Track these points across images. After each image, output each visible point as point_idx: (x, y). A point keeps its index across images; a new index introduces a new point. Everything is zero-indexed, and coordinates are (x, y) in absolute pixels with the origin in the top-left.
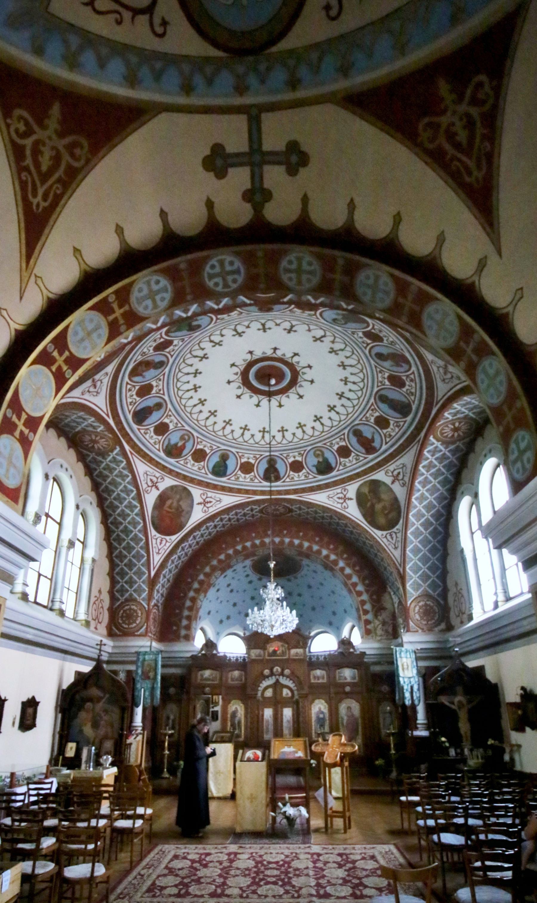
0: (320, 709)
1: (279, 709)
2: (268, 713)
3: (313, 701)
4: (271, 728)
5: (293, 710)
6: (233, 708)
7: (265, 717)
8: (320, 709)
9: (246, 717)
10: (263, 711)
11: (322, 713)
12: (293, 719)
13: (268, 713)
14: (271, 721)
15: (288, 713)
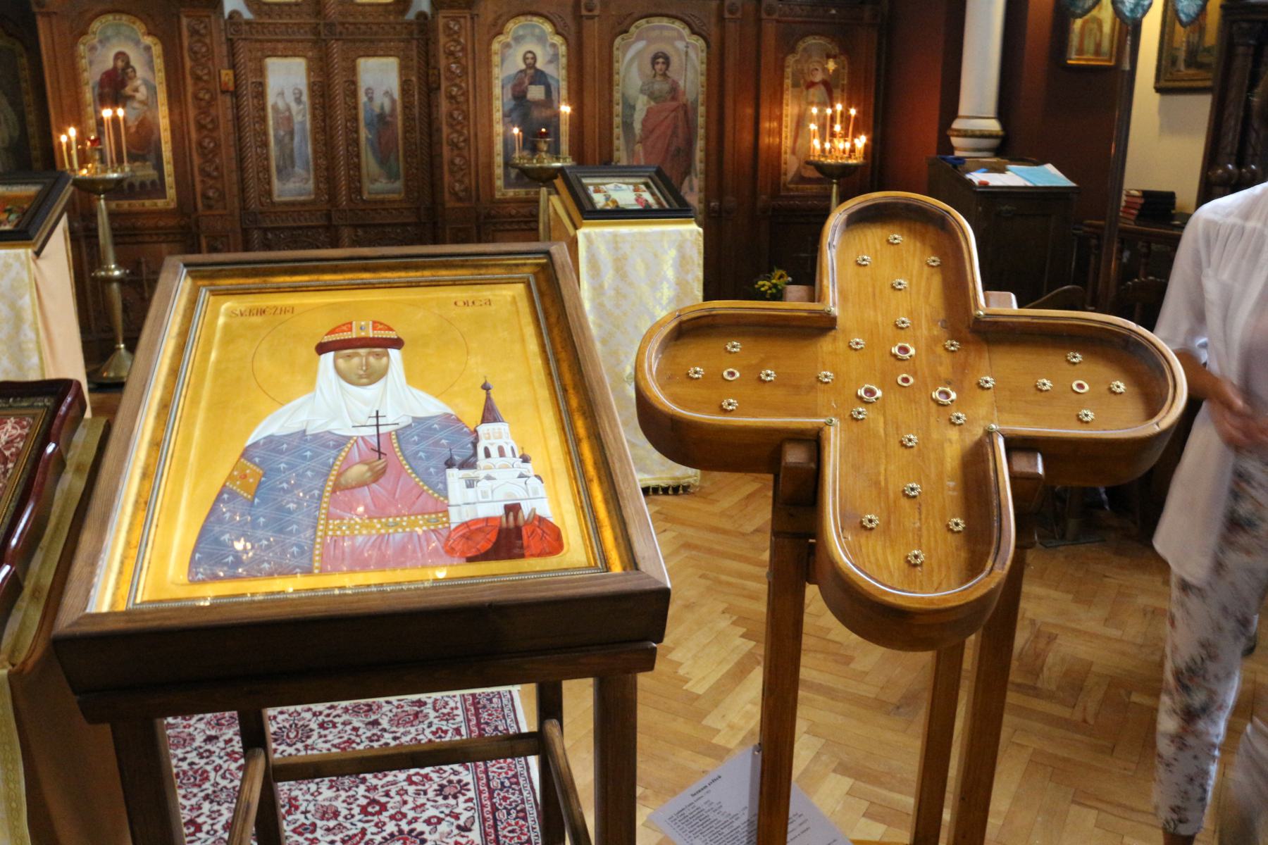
0: (530, 59)
1: (337, 58)
2: (286, 79)
3: (497, 29)
4: (304, 147)
5: (403, 68)
6: (107, 61)
7: (271, 98)
8: (530, 59)
9: (175, 96)
10: (261, 71)
11: (539, 77)
12: (407, 107)
13: (286, 79)
14: (302, 116)
15: (380, 77)
